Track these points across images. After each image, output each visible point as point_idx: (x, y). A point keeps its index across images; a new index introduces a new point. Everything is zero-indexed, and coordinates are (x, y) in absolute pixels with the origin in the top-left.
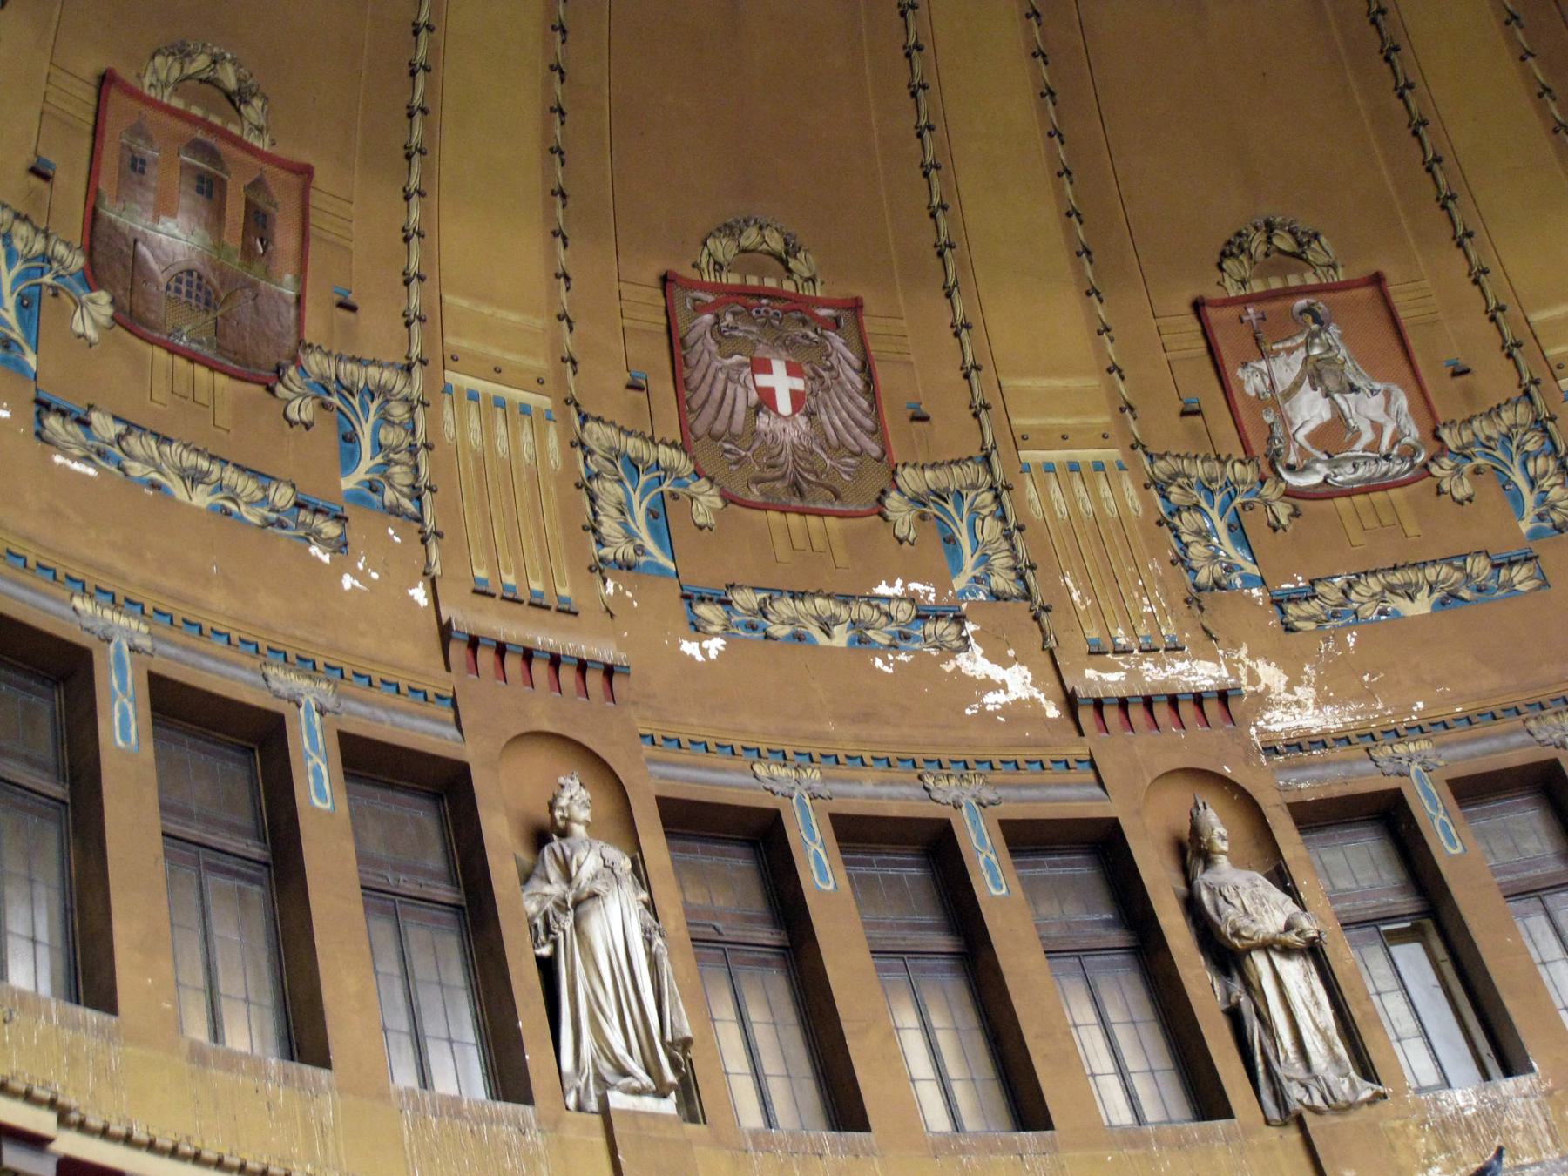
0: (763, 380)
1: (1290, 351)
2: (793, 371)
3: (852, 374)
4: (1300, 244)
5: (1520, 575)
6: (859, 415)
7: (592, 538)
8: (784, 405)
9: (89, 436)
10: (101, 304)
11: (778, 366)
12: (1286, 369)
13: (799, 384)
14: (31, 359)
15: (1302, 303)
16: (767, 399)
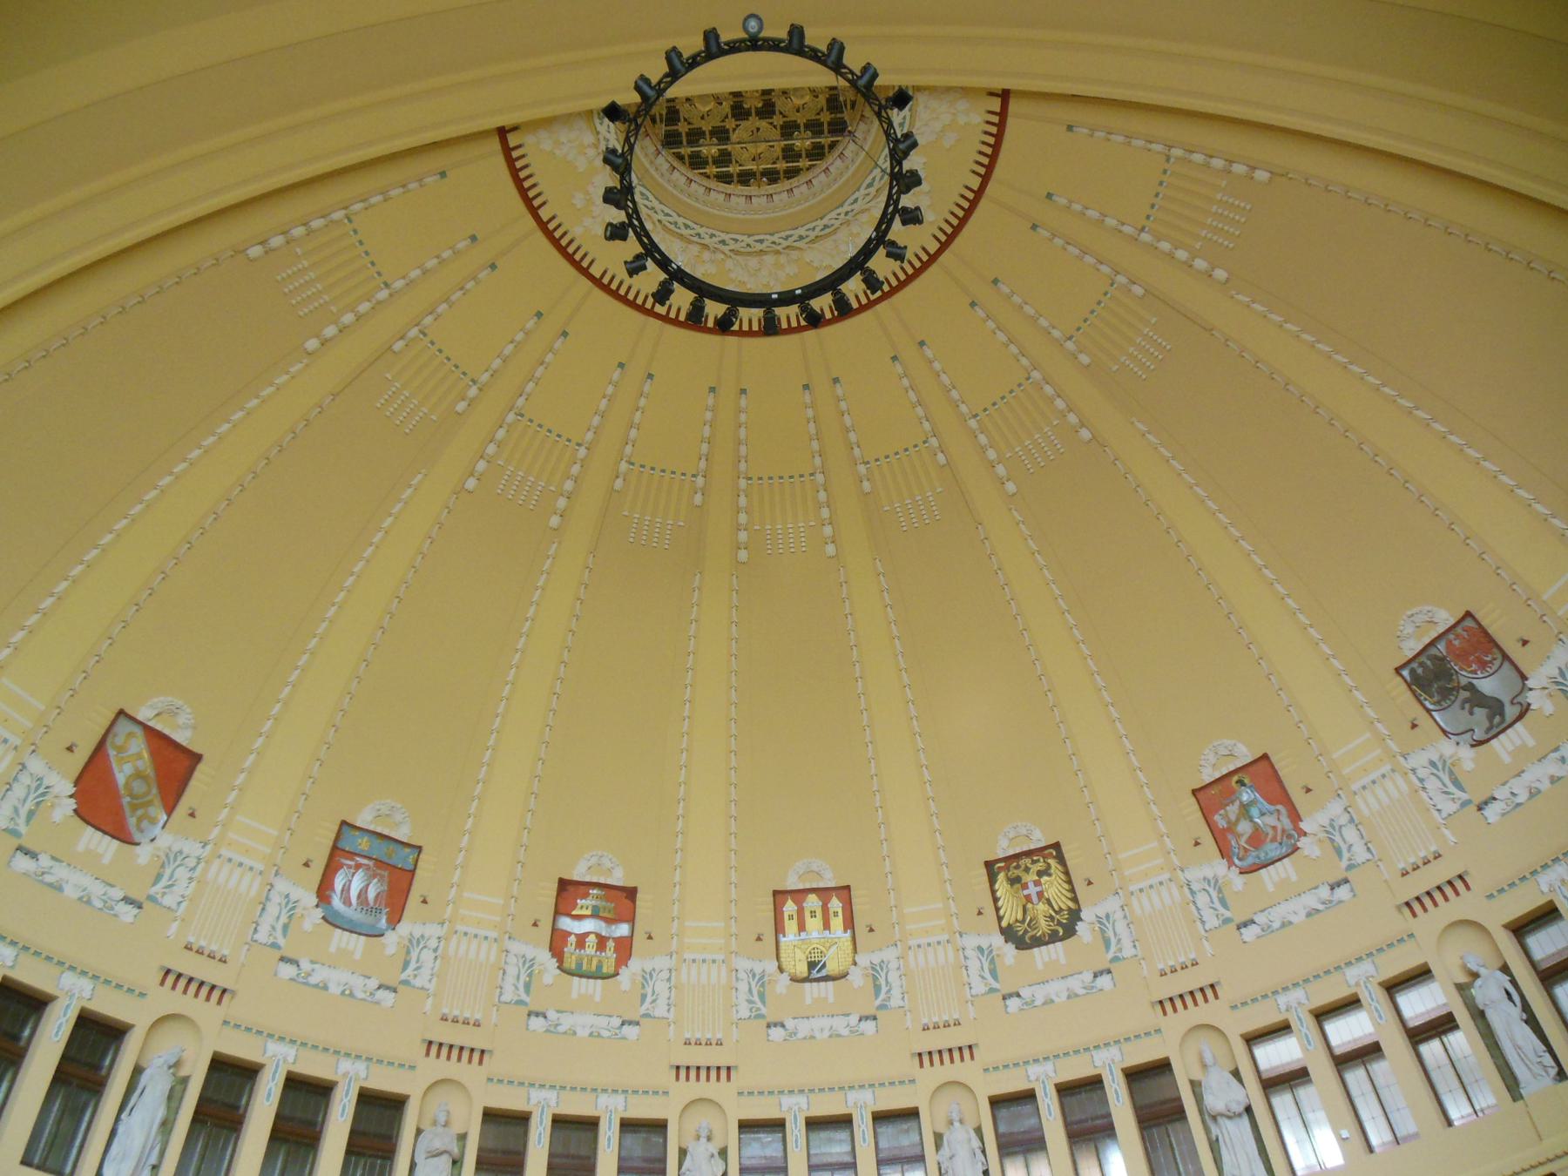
0: (1026, 892)
1: (1232, 802)
2: (1037, 883)
3: (1059, 873)
4: (1230, 751)
5: (1343, 893)
6: (1061, 890)
7: (967, 987)
8: (1035, 898)
9: (786, 1030)
10: (785, 978)
11: (1031, 885)
12: (1233, 810)
13: (1038, 889)
14: (764, 1011)
15: (1235, 778)
16: (1028, 898)
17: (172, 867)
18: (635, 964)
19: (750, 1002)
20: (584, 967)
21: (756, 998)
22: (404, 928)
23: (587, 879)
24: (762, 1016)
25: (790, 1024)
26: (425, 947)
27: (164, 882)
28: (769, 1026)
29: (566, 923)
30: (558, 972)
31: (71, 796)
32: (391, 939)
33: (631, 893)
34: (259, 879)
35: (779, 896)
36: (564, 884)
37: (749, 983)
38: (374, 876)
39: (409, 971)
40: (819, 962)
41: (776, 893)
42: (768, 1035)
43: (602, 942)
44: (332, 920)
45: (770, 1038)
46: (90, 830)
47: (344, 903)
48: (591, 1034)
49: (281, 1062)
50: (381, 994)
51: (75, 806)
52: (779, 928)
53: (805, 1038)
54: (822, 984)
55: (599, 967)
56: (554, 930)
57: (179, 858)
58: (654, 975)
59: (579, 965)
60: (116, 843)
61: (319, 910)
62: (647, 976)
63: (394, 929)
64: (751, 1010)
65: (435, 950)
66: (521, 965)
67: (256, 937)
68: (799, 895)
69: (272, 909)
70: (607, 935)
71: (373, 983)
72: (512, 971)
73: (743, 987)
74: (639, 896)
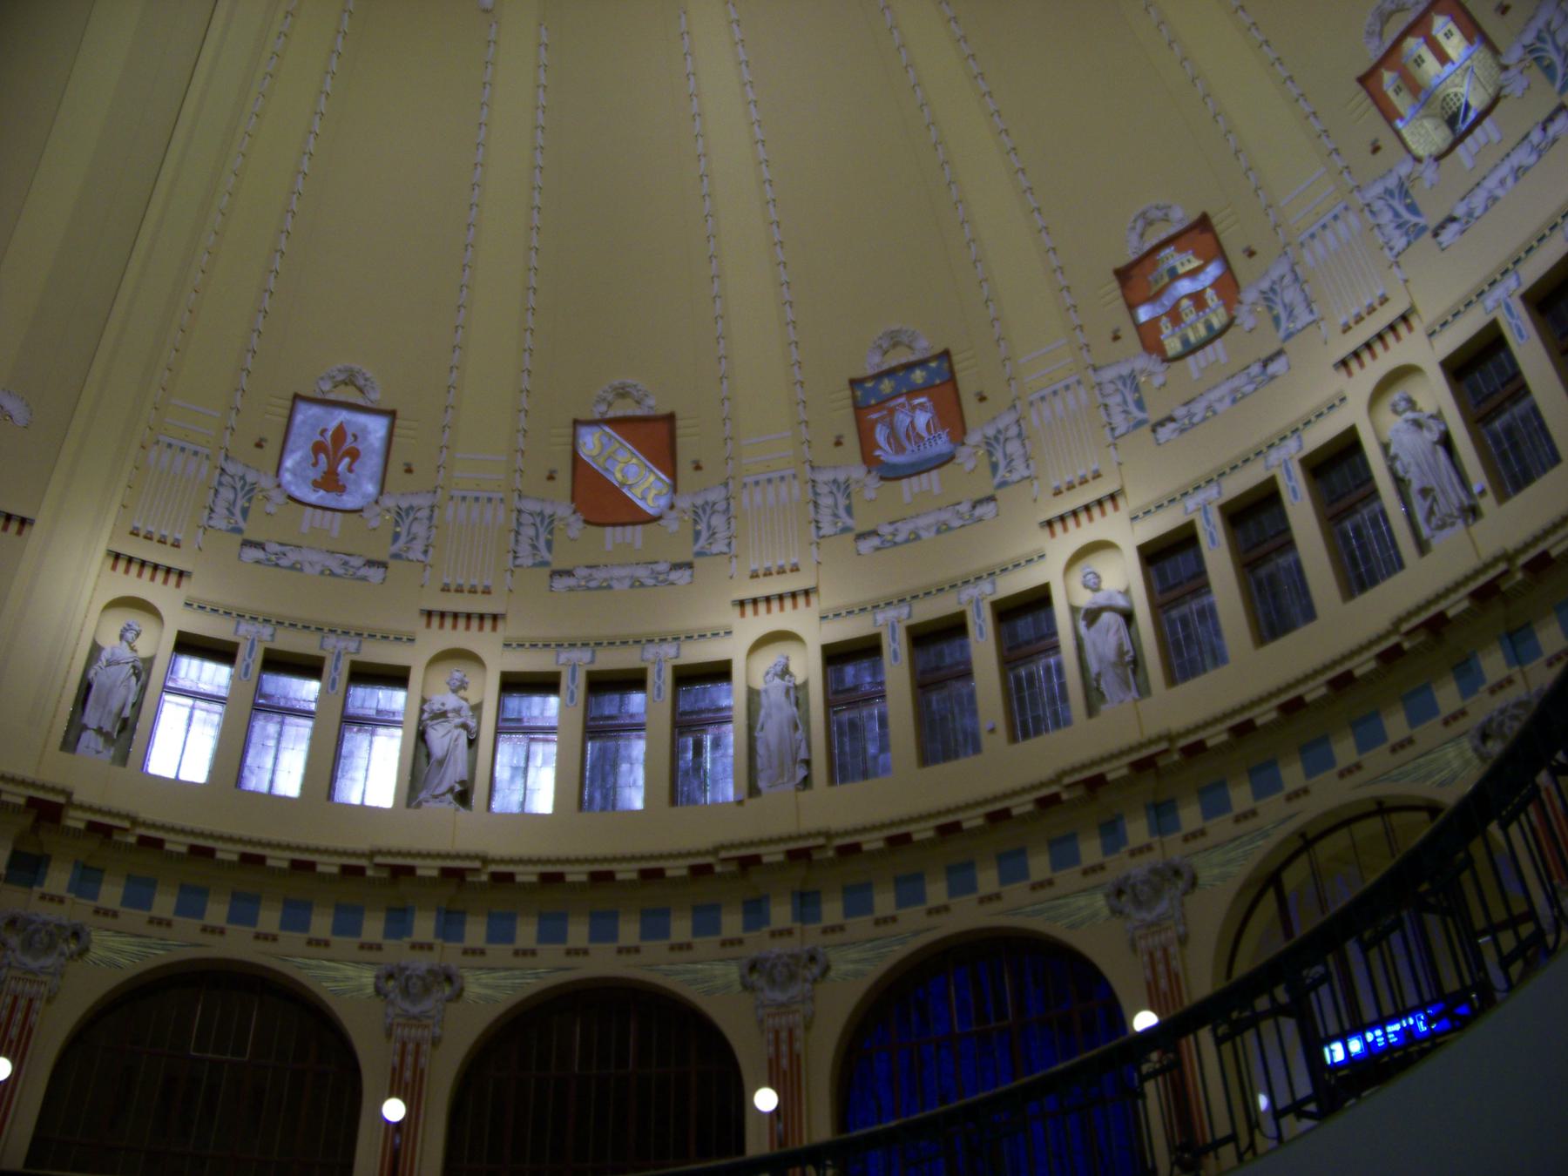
14: (1422, 221)
17: (705, 519)
18: (1249, 296)
19: (1399, 227)
20: (1192, 338)
21: (1406, 215)
22: (973, 438)
23: (1147, 247)
24: (1424, 229)
25: (1460, 211)
26: (1006, 440)
27: (705, 534)
28: (1436, 235)
29: (1144, 314)
30: (1166, 365)
31: (574, 512)
32: (963, 452)
33: (1203, 224)
34: (796, 483)
35: (1368, 80)
36: (1124, 275)
37: (1391, 207)
38: (914, 408)
39: (1001, 471)
40: (1459, 109)
41: (1362, 80)
42: (1440, 244)
43: (1198, 299)
44: (892, 474)
45: (1444, 245)
46: (609, 530)
47: (897, 452)
48: (1234, 401)
49: (896, 624)
50: (979, 511)
51: (582, 518)
52: (1389, 114)
53: (1486, 209)
54: (1478, 132)
55: (1209, 327)
56: (1139, 327)
57: (708, 509)
58: (1276, 287)
59: (1185, 341)
60: (639, 528)
61: (874, 473)
62: (1268, 297)
63: (963, 444)
64: (1407, 233)
65: (1020, 435)
66: (1120, 386)
67: (822, 533)
68: (1391, 56)
69: (826, 501)
70: (1200, 288)
71: (964, 508)
72: (1114, 401)
73: (1386, 217)
74: (1214, 221)
